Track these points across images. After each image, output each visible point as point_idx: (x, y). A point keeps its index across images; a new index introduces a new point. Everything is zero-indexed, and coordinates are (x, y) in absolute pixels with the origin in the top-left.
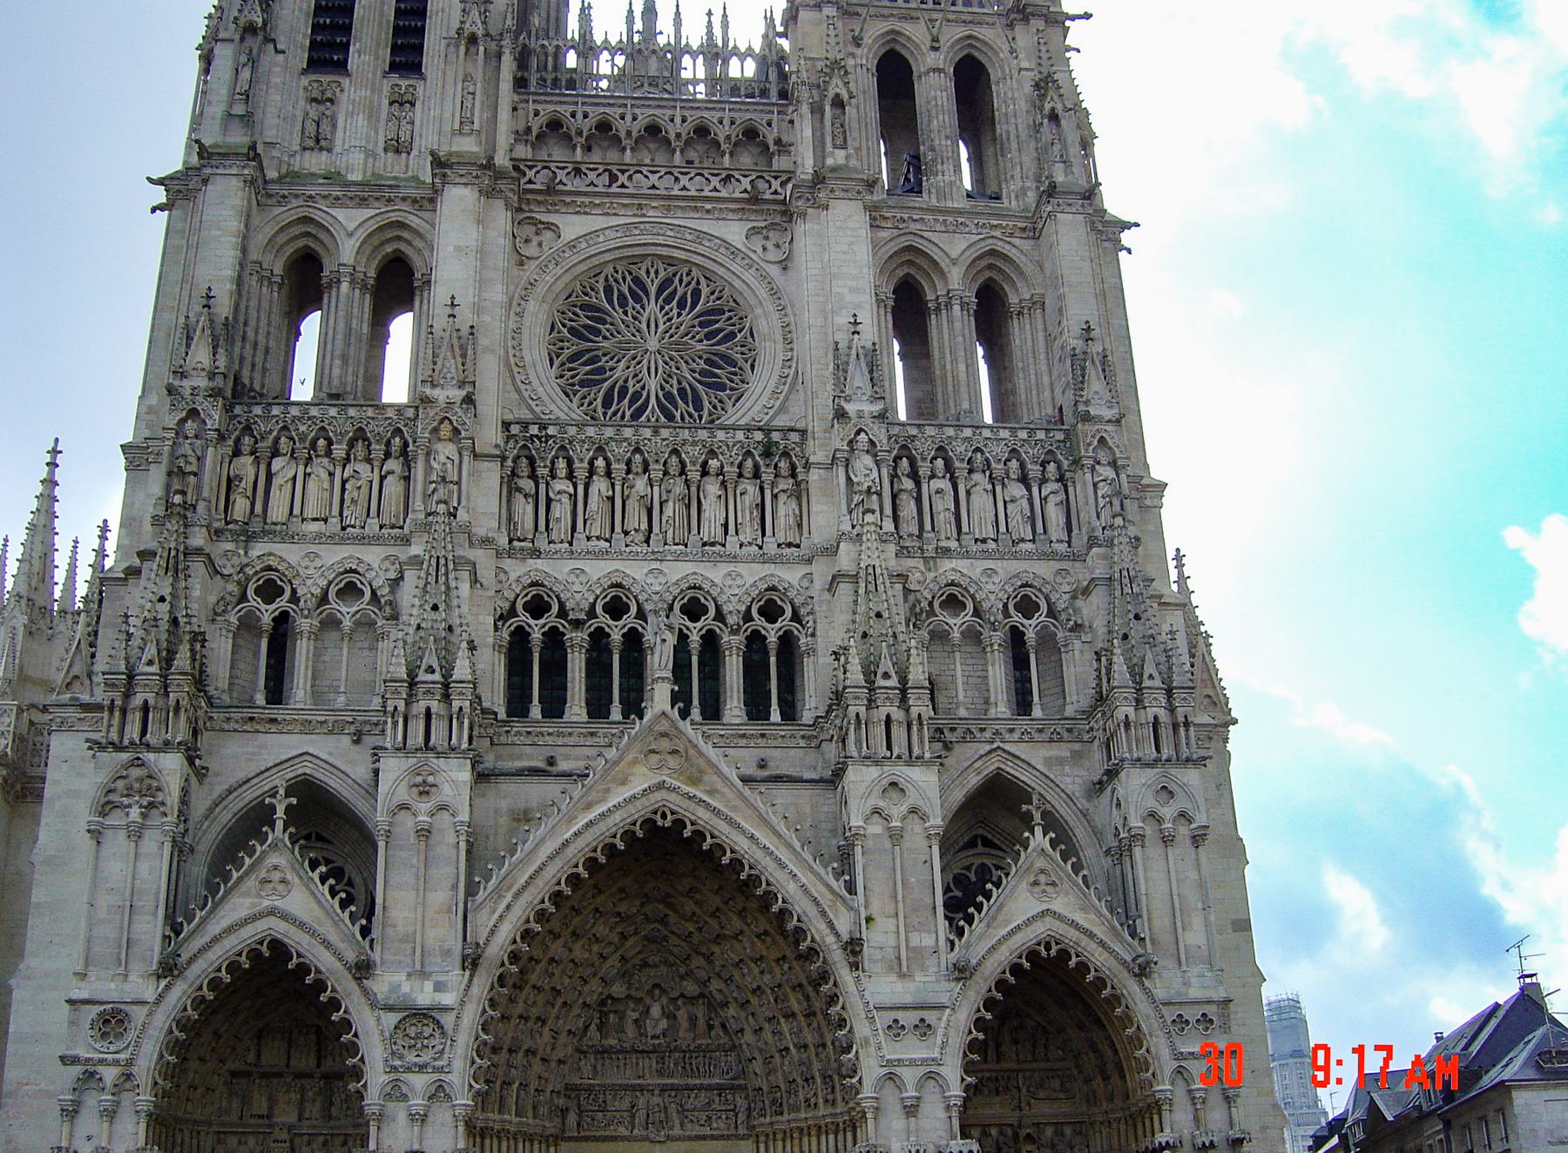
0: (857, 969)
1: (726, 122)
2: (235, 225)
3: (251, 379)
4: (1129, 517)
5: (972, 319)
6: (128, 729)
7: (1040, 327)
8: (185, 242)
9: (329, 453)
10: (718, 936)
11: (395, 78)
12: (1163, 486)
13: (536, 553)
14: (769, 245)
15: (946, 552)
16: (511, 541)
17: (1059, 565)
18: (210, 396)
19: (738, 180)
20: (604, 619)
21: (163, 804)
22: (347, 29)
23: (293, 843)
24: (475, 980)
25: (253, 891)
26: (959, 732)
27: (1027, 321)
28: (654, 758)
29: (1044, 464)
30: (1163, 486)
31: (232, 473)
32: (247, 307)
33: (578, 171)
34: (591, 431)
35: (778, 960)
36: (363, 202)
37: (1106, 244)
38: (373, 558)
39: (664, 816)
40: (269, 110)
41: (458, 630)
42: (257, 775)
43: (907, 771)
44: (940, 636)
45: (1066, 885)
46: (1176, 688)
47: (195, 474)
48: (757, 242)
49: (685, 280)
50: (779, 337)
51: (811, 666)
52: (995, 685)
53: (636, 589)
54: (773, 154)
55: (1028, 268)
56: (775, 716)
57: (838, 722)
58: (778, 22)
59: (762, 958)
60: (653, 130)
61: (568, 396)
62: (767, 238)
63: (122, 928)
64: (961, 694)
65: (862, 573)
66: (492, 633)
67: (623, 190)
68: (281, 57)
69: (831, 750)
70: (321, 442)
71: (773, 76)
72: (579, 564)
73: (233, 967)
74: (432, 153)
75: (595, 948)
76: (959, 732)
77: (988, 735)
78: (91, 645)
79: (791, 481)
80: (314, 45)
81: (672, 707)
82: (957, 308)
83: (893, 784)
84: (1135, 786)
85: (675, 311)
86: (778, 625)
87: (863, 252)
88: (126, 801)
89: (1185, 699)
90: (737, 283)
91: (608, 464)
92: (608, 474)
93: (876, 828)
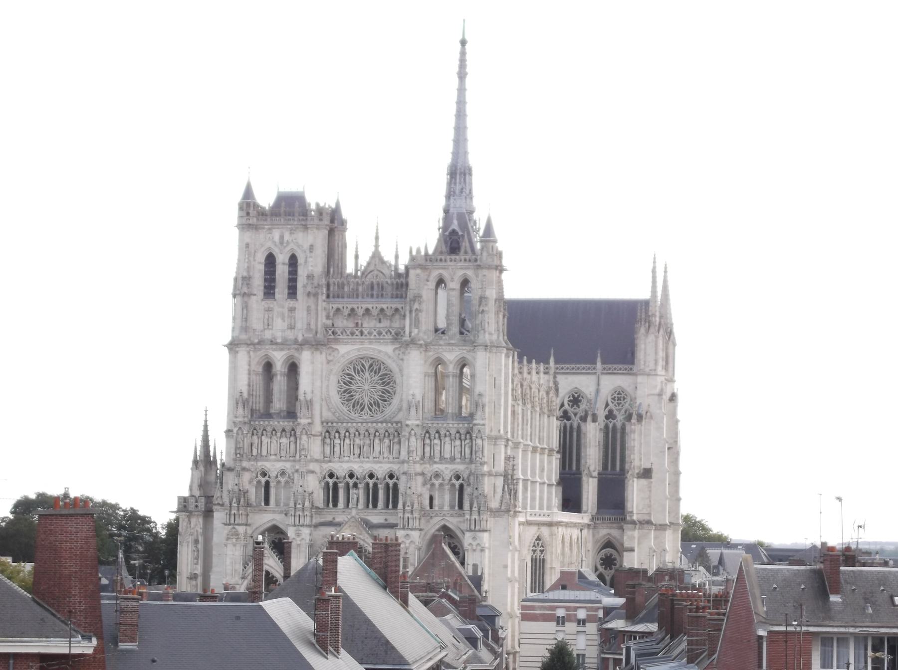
9: (276, 435)
13: (330, 461)
15: (436, 463)
16: (324, 457)
20: (348, 479)
26: (434, 514)
28: (351, 528)
36: (282, 350)
44: (433, 485)
67: (357, 337)
76: (434, 514)
83: (407, 535)
91: (350, 434)
92: (349, 436)
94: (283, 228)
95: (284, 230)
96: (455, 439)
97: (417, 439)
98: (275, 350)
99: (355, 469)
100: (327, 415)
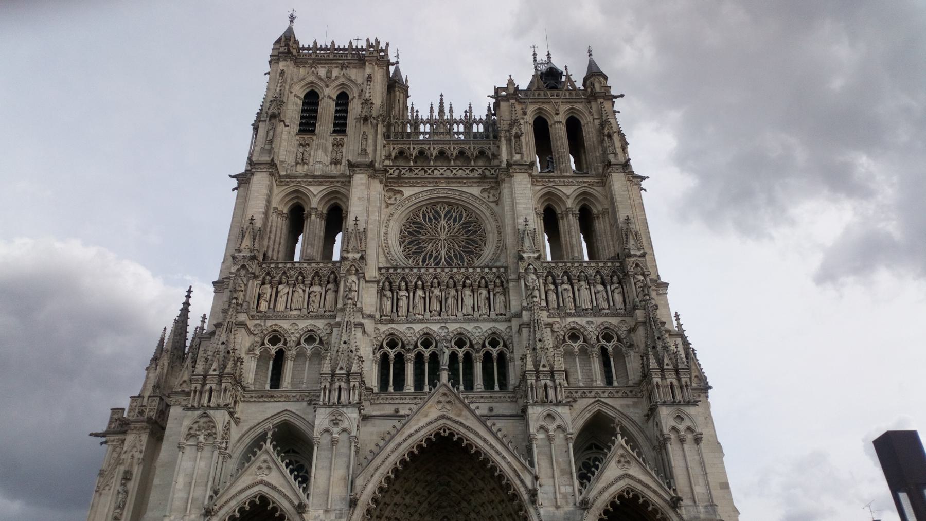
0: (535, 504)
1: (472, 148)
2: (266, 192)
3: (272, 255)
4: (652, 296)
5: (578, 221)
6: (202, 401)
7: (607, 221)
8: (244, 200)
9: (303, 282)
10: (473, 491)
11: (335, 136)
12: (666, 285)
13: (392, 321)
14: (491, 196)
15: (570, 315)
16: (381, 317)
17: (620, 319)
18: (251, 259)
19: (477, 170)
20: (421, 348)
21: (215, 434)
22: (315, 118)
23: (274, 449)
24: (356, 512)
25: (254, 472)
26: (579, 394)
27: (601, 220)
28: (440, 406)
29: (611, 277)
30: (666, 285)
31: (260, 292)
32: (271, 226)
33: (411, 170)
34: (415, 270)
35: (500, 502)
36: (321, 184)
37: (635, 186)
38: (320, 324)
39: (445, 431)
40: (282, 148)
41: (355, 352)
42: (263, 421)
43: (554, 408)
45: (634, 463)
46: (680, 369)
47: (242, 291)
48: (485, 195)
49: (456, 211)
50: (495, 231)
51: (512, 367)
52: (595, 372)
53: (434, 335)
54: (491, 160)
55: (601, 198)
56: (497, 388)
57: (524, 388)
58: (492, 109)
59: (493, 501)
60: (442, 153)
61: (407, 258)
62: (489, 193)
63: (189, 494)
64: (579, 377)
65: (532, 323)
66: (372, 355)
68: (287, 128)
69: (521, 402)
70: (300, 278)
71: (491, 129)
72: (410, 325)
73: (241, 510)
74: (348, 161)
75: (417, 498)
76: (579, 394)
77: (593, 394)
78: (193, 367)
79: (501, 288)
80: (301, 124)
81: (449, 381)
82: (571, 216)
84: (666, 415)
85: (452, 223)
86: (497, 349)
87: (529, 193)
88: (198, 432)
89: (684, 374)
90: (477, 211)
91: (423, 283)
93: (541, 436)
94: (331, 63)
95: (333, 66)
96: (596, 283)
97: (538, 278)
98: (310, 184)
99: (435, 332)
100: (383, 263)
